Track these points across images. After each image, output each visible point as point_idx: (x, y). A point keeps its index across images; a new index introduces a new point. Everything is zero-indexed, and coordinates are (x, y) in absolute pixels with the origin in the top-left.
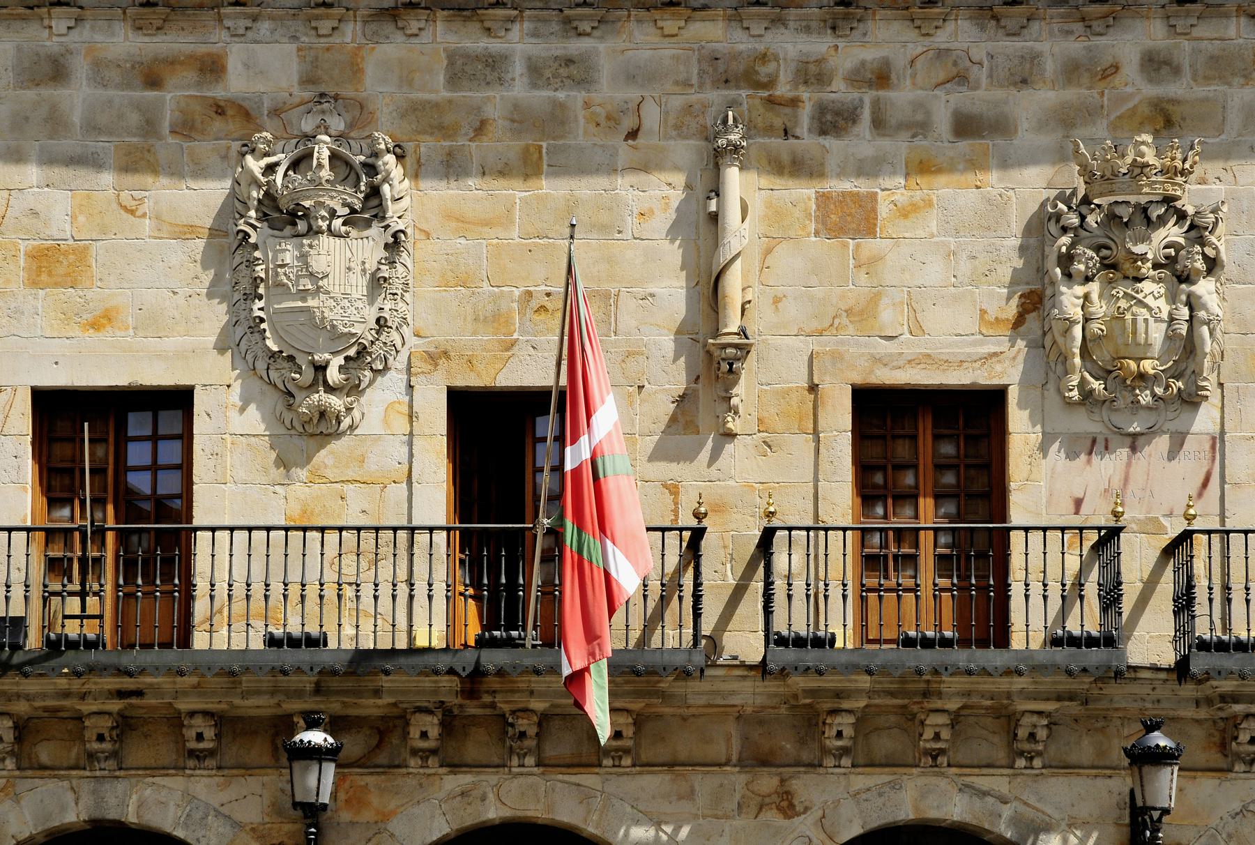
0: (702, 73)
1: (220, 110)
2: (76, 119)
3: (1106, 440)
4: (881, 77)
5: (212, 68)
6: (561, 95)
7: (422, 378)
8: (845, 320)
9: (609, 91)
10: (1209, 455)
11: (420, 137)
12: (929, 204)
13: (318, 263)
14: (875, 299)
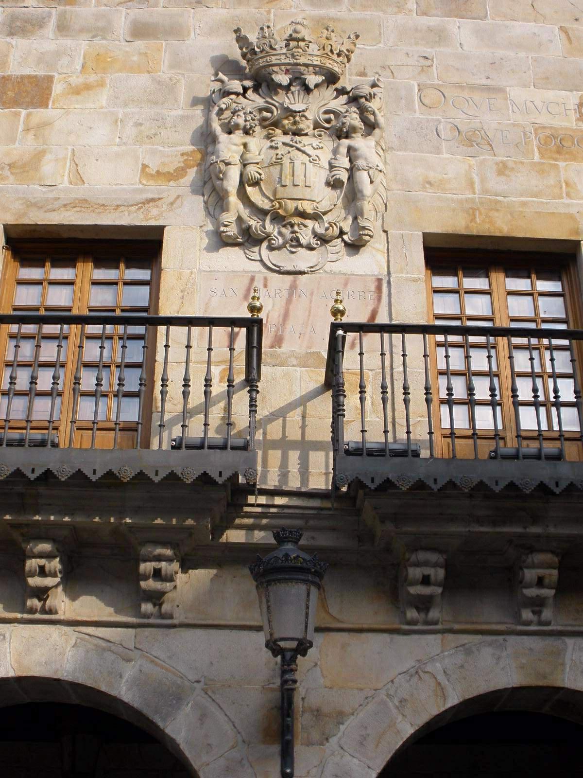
3: (266, 279)
10: (374, 296)
12: (101, 84)
14: (39, 156)
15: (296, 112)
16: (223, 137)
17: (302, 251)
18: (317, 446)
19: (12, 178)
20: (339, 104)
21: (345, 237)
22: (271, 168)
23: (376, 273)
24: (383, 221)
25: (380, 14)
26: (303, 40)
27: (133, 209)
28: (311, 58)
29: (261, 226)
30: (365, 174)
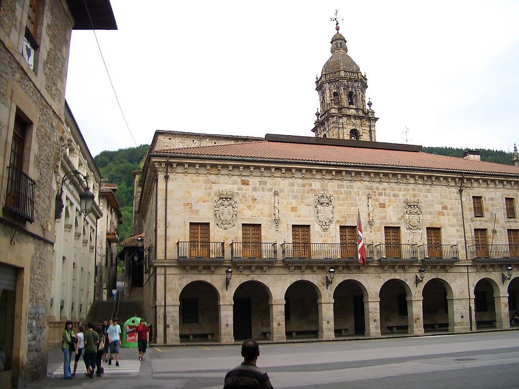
2: (296, 191)
5: (311, 185)
9: (355, 190)
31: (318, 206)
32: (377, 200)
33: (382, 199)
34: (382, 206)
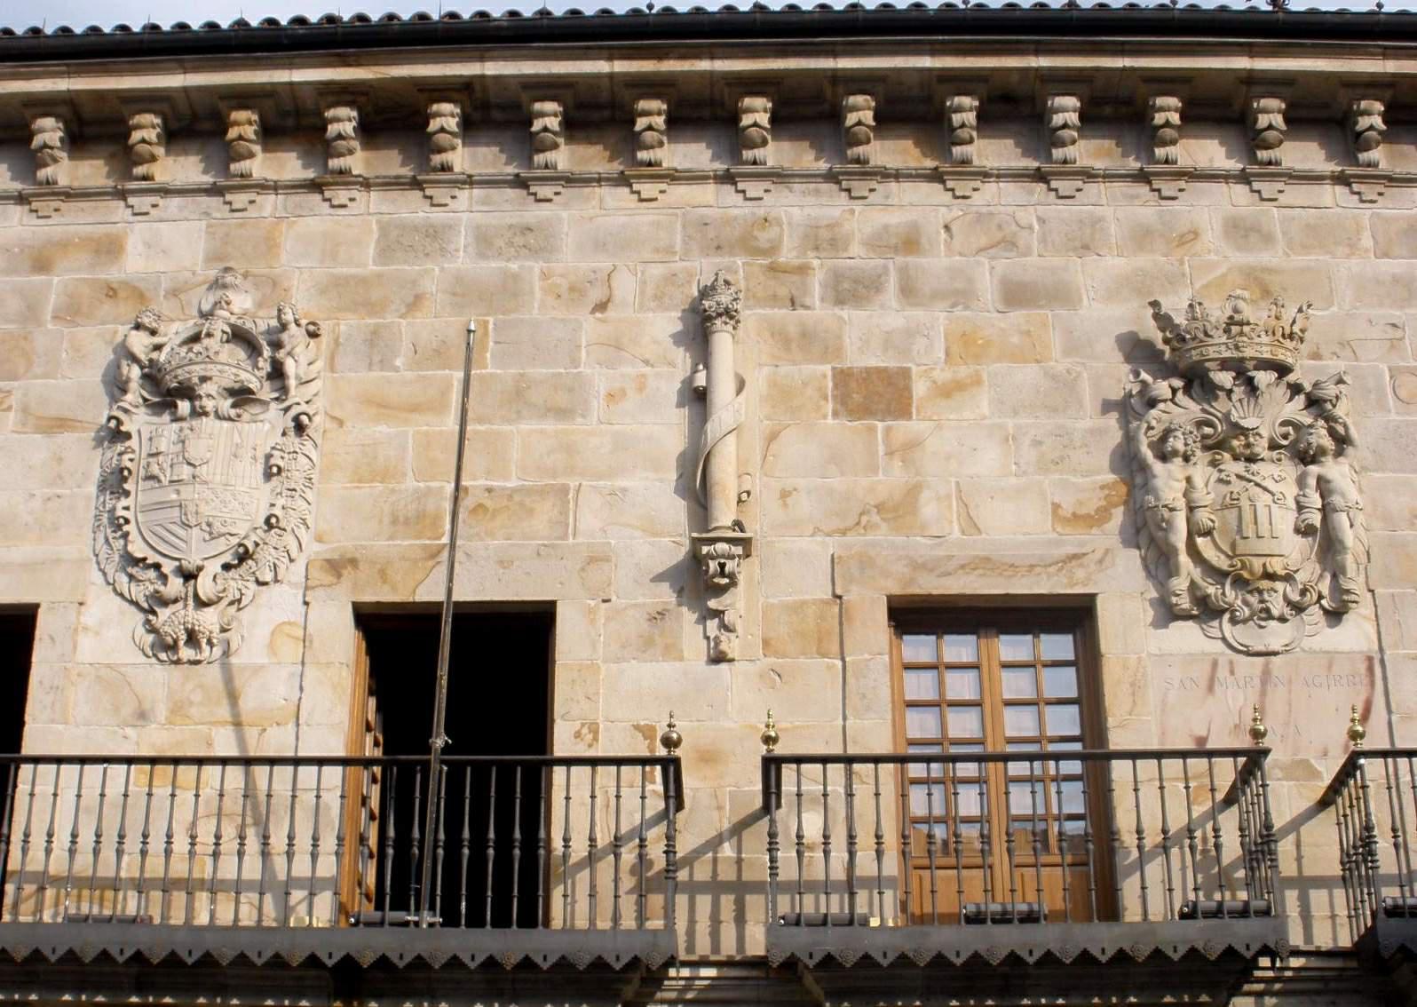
0: (687, 239)
1: (111, 292)
3: (1231, 663)
4: (910, 243)
5: (110, 248)
6: (514, 266)
7: (320, 592)
8: (876, 518)
9: (571, 260)
10: (1366, 681)
11: (339, 315)
12: (977, 382)
13: (196, 450)
14: (913, 492)
15: (1248, 429)
16: (1158, 467)
17: (1273, 623)
18: (1322, 882)
19: (884, 526)
20: (1295, 409)
21: (1324, 602)
22: (1226, 512)
23: (1365, 649)
24: (1367, 577)
25: (1327, 257)
26: (1248, 324)
27: (1051, 569)
28: (1258, 348)
29: (1221, 593)
30: (1344, 515)
31: (139, 422)
32: (808, 342)
33: (866, 336)
34: (876, 395)
